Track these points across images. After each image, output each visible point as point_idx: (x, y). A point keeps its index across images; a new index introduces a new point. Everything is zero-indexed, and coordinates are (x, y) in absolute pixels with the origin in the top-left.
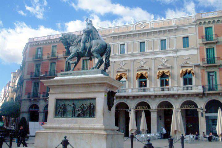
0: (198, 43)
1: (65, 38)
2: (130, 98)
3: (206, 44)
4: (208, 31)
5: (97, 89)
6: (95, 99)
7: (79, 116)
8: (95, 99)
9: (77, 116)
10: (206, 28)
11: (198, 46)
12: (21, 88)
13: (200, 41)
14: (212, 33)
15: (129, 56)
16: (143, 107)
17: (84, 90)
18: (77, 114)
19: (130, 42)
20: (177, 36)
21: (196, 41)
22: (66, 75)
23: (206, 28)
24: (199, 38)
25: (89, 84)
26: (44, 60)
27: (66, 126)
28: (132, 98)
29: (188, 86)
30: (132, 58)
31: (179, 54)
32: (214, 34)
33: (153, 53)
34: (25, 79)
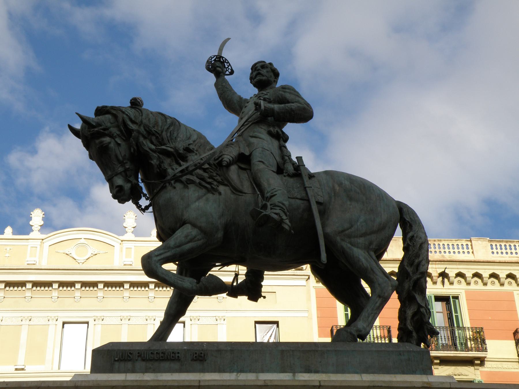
1: (129, 132)
22: (166, 365)
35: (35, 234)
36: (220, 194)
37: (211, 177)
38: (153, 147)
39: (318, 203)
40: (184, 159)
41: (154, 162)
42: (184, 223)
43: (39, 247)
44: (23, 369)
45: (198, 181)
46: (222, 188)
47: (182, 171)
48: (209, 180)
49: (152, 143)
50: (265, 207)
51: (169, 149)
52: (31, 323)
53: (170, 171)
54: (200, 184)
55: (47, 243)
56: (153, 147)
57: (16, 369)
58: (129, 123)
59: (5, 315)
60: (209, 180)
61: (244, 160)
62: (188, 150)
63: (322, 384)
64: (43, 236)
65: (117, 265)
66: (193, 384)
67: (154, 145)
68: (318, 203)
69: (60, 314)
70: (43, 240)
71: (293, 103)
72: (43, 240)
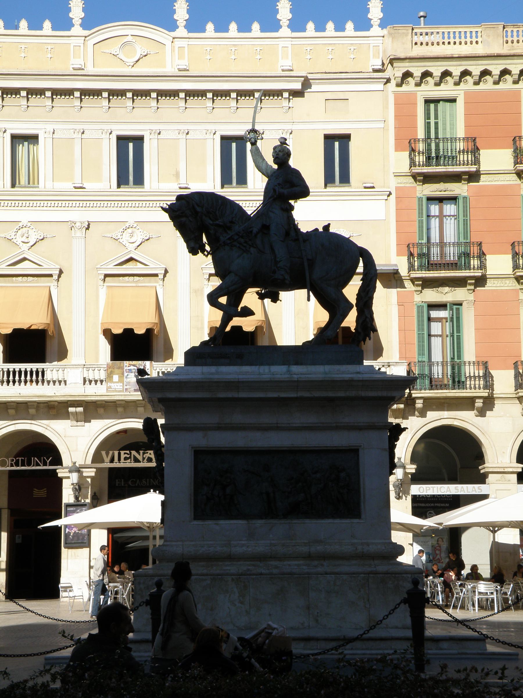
2: (71, 410)
3: (428, 179)
4: (436, 117)
8: (354, 452)
10: (428, 102)
11: (392, 184)
13: (401, 161)
14: (453, 126)
15: (57, 200)
16: (134, 453)
17: (311, 419)
19: (64, 131)
20: (294, 127)
23: (428, 102)
24: (398, 148)
27: (244, 548)
28: (80, 409)
30: (80, 216)
32: (461, 133)
35: (77, 30)
36: (251, 254)
37: (246, 242)
38: (211, 222)
39: (308, 260)
40: (230, 228)
41: (212, 232)
42: (230, 272)
43: (82, 45)
44: (81, 188)
45: (238, 245)
46: (252, 250)
47: (229, 239)
48: (245, 244)
49: (210, 219)
50: (274, 272)
51: (221, 223)
52: (84, 136)
53: (221, 237)
54: (239, 247)
55: (91, 42)
56: (211, 222)
57: (75, 188)
58: (196, 207)
59: (56, 126)
60: (245, 244)
61: (265, 228)
62: (232, 222)
63: (299, 379)
64: (86, 33)
65: (170, 69)
66: (235, 380)
67: (212, 220)
68: (308, 260)
69: (113, 127)
70: (86, 37)
71: (297, 186)
72: (86, 37)
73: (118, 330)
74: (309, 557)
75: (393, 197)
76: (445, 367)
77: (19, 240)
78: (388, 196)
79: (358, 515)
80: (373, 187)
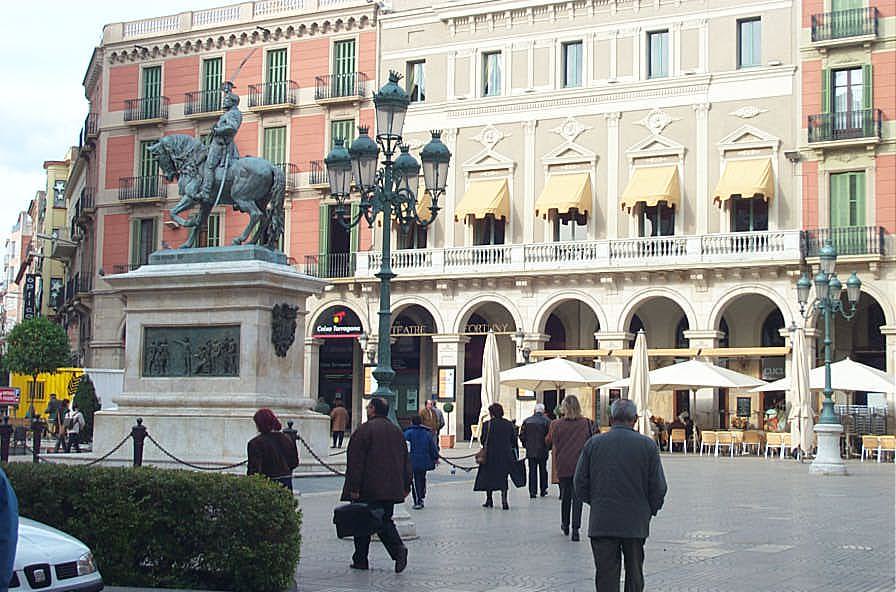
0: (799, 46)
5: (243, 302)
6: (239, 326)
7: (200, 372)
9: (195, 371)
12: (86, 239)
17: (210, 304)
18: (194, 369)
19: (521, 42)
21: (793, 33)
25: (222, 288)
26: (173, 123)
29: (752, 234)
31: (719, 92)
33: (614, 90)
34: (103, 206)
52: (536, 47)
73: (480, 215)
74: (202, 405)
75: (799, 72)
76: (833, 234)
77: (485, 141)
78: (795, 71)
79: (236, 374)
80: (780, 65)
